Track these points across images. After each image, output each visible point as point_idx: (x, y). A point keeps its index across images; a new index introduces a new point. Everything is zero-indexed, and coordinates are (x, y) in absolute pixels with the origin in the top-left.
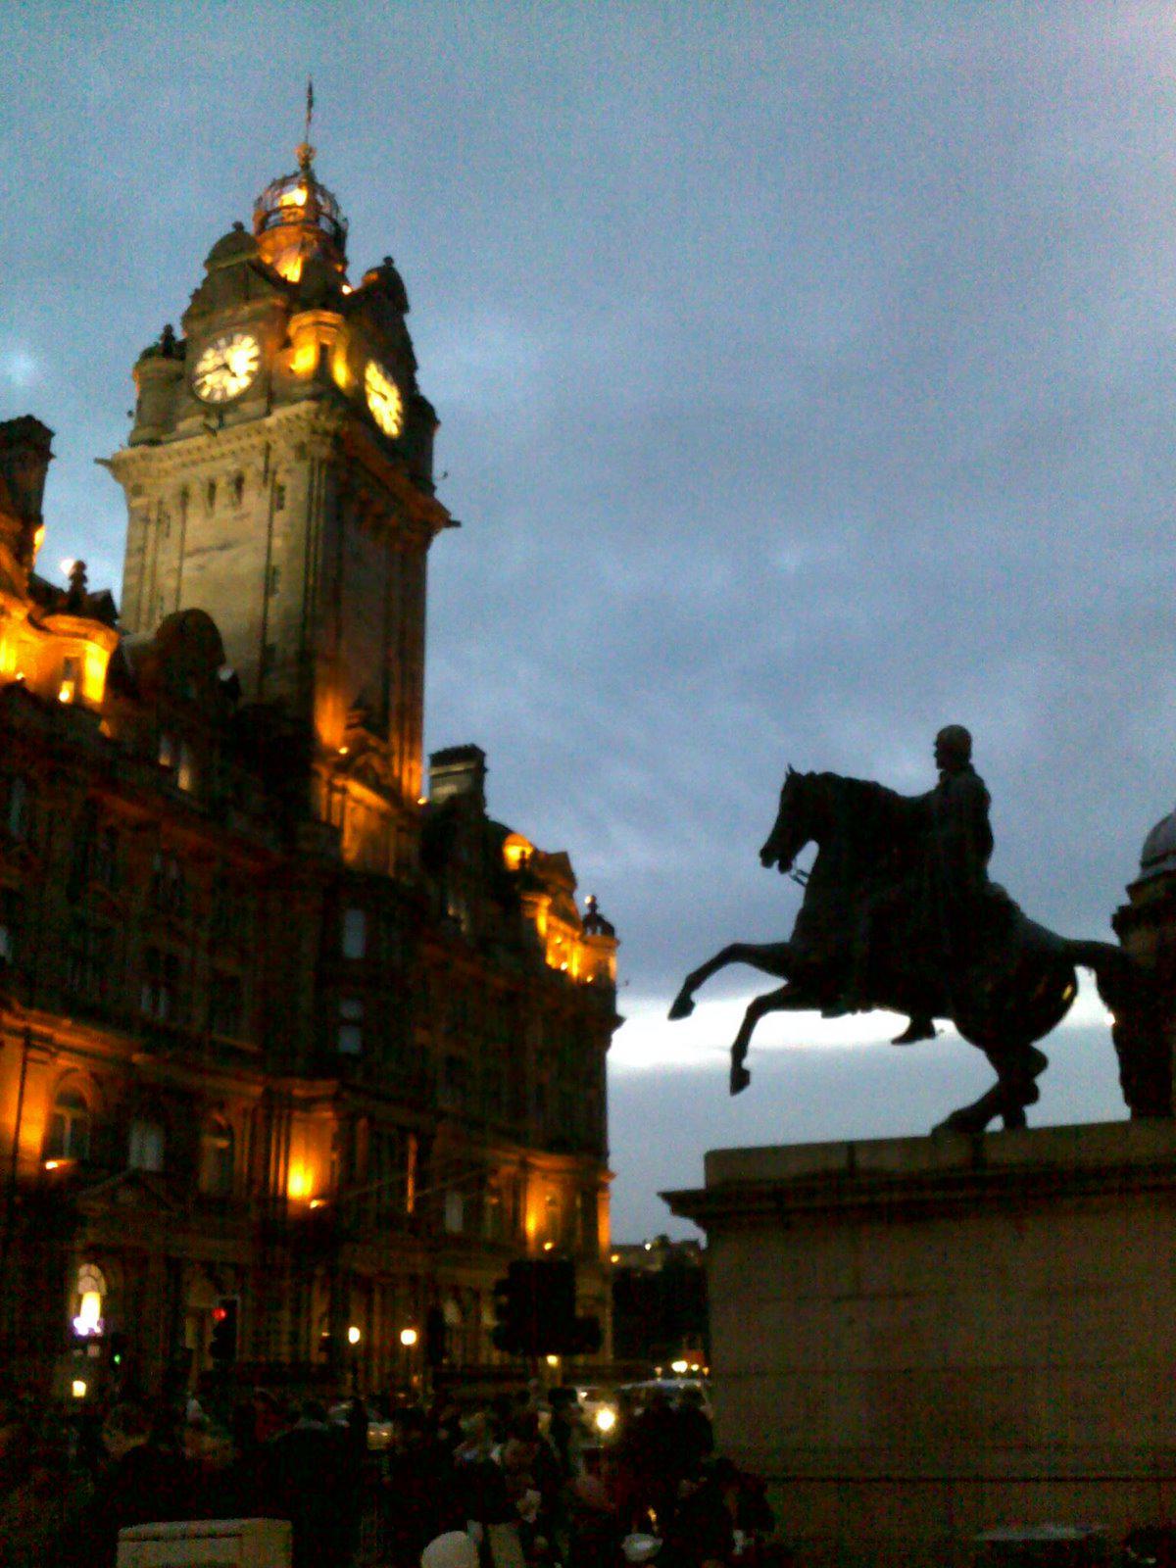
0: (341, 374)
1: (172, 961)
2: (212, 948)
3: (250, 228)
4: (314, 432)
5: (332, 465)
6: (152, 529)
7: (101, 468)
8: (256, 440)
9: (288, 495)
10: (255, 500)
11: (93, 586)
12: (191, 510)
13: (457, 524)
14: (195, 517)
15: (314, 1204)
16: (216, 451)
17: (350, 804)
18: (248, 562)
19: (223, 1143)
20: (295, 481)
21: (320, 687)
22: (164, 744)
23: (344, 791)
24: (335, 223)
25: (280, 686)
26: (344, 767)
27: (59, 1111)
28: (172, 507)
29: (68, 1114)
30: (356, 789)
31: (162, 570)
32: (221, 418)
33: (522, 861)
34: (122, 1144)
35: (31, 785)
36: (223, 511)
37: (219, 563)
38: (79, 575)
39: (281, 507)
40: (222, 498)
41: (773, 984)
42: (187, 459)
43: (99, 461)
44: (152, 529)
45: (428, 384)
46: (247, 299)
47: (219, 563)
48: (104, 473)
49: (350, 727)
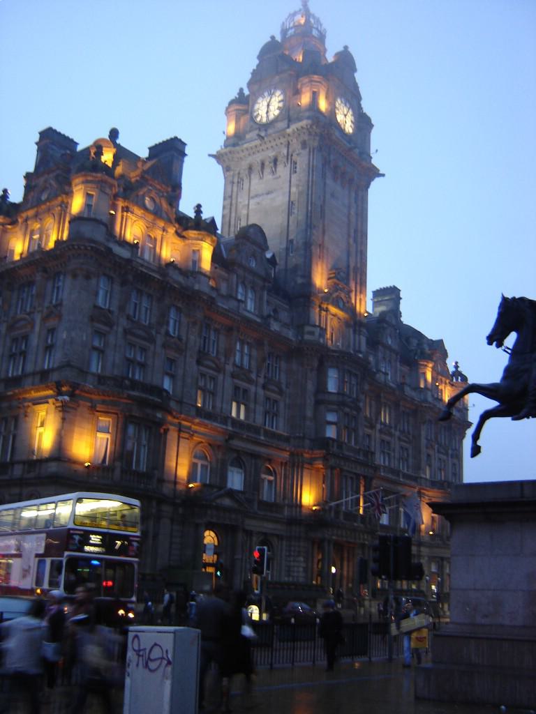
0: (323, 105)
1: (245, 391)
2: (264, 387)
3: (278, 38)
5: (320, 149)
6: (235, 185)
7: (211, 158)
8: (283, 140)
10: (283, 171)
11: (205, 215)
12: (253, 176)
13: (383, 175)
15: (314, 508)
17: (330, 317)
18: (280, 200)
19: (272, 478)
20: (302, 160)
21: (314, 261)
22: (240, 290)
23: (327, 310)
24: (319, 31)
25: (295, 259)
27: (195, 461)
28: (244, 174)
30: (333, 310)
31: (240, 206)
34: (224, 478)
35: (178, 310)
36: (268, 176)
38: (198, 209)
39: (296, 172)
40: (267, 170)
41: (492, 404)
43: (210, 155)
44: (235, 185)
45: (367, 107)
48: (213, 161)
49: (329, 279)
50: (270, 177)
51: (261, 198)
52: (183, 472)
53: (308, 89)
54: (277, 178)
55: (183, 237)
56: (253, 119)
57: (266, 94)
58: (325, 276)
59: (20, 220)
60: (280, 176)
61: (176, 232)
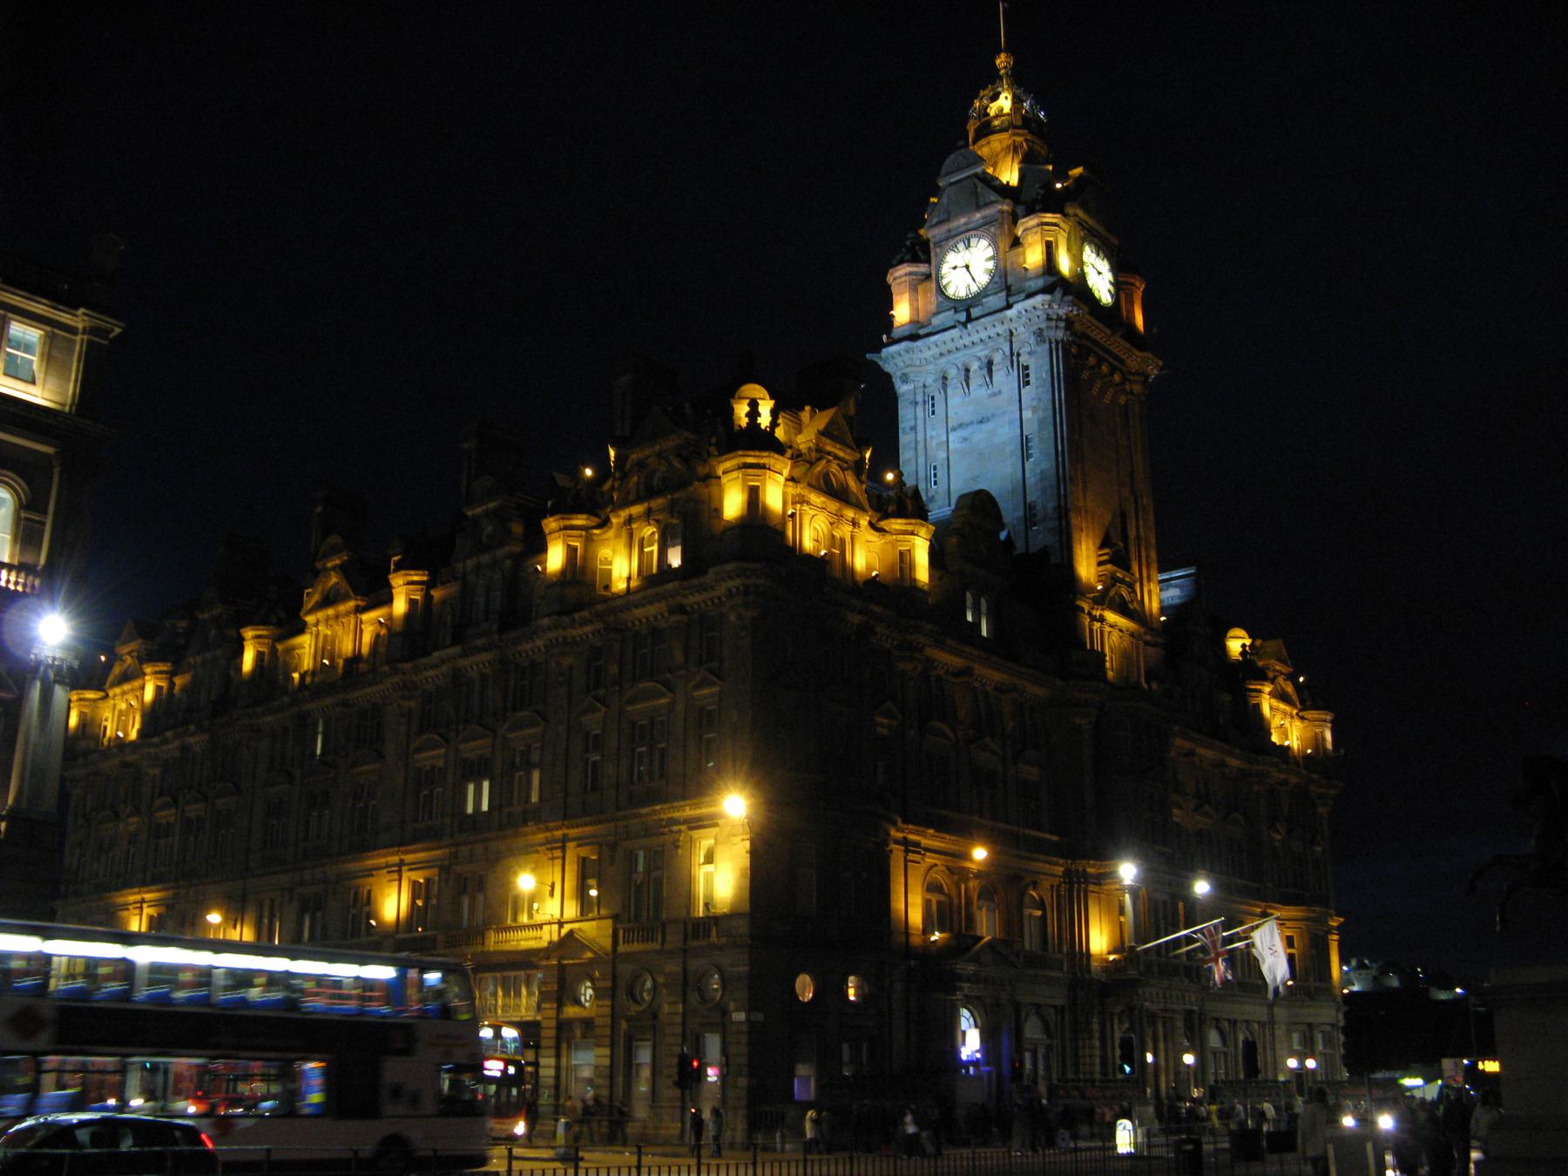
0: (1065, 265)
4: (1049, 319)
6: (920, 409)
8: (1000, 329)
9: (1031, 372)
10: (1005, 379)
14: (956, 397)
15: (1111, 957)
16: (967, 341)
18: (1006, 432)
20: (1039, 363)
21: (1076, 536)
23: (1102, 620)
25: (1041, 537)
26: (1102, 600)
27: (929, 896)
28: (934, 389)
29: (934, 898)
30: (1111, 617)
31: (933, 444)
32: (968, 311)
33: (1243, 653)
37: (980, 435)
39: (1028, 383)
40: (977, 378)
42: (944, 349)
44: (920, 409)
46: (978, 208)
47: (980, 435)
49: (1100, 564)
50: (983, 392)
51: (970, 429)
52: (916, 917)
53: (1037, 237)
54: (994, 395)
56: (941, 291)
57: (961, 246)
58: (1093, 561)
59: (614, 520)
61: (871, 524)
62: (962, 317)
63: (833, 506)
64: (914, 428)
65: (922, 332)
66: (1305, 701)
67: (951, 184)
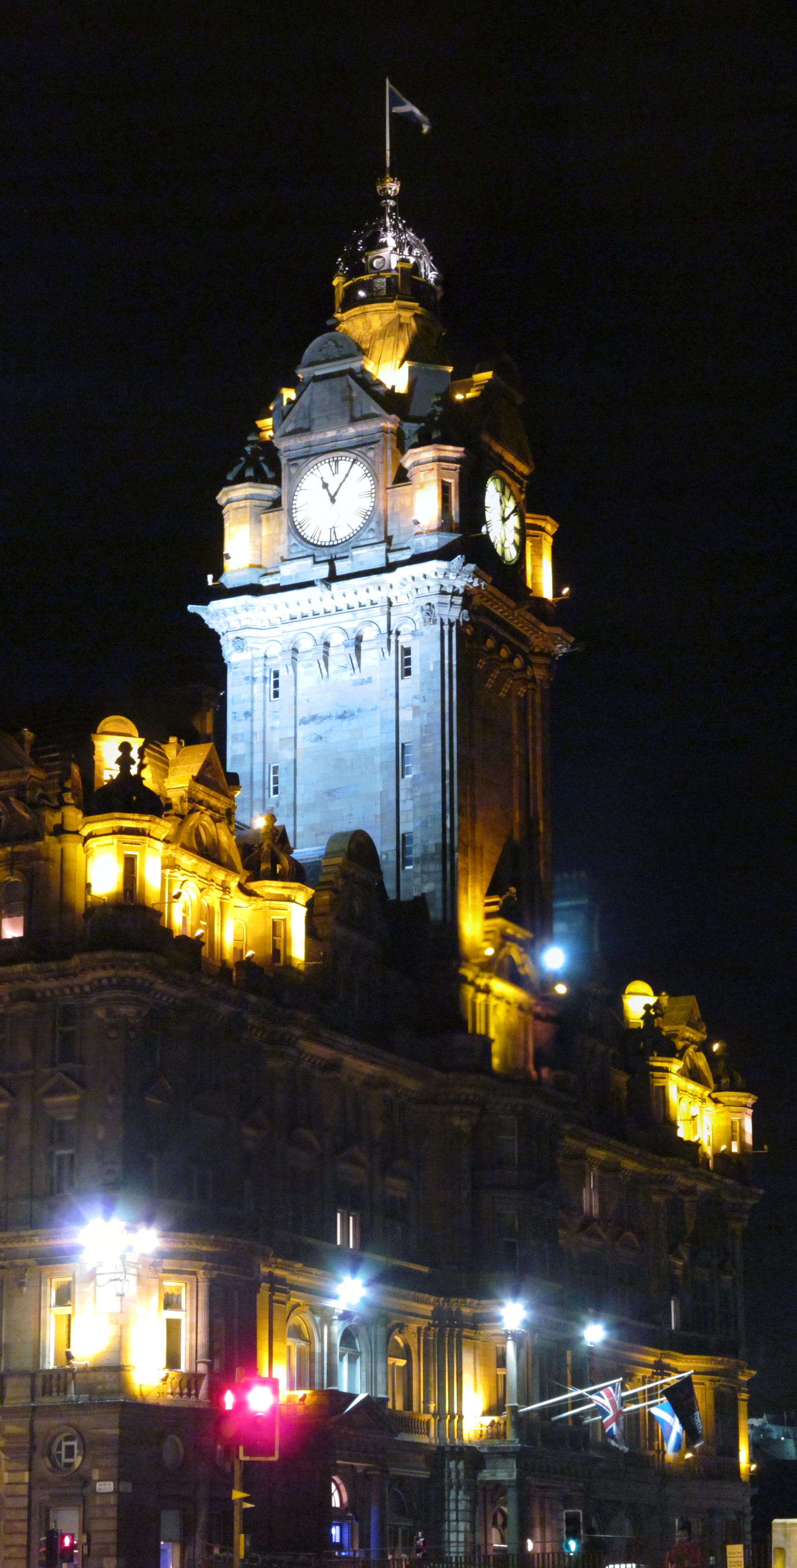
5: (461, 628)
6: (258, 688)
9: (414, 656)
10: (377, 662)
17: (493, 1002)
20: (428, 651)
23: (487, 991)
30: (499, 986)
31: (274, 738)
32: (331, 562)
33: (647, 1018)
39: (408, 672)
44: (258, 688)
46: (354, 420)
47: (340, 734)
49: (488, 916)
50: (347, 676)
53: (433, 477)
55: (250, 893)
56: (294, 530)
58: (482, 910)
60: (370, 680)
61: (241, 887)
62: (323, 571)
63: (204, 867)
64: (248, 714)
65: (266, 582)
66: (722, 1077)
67: (316, 379)
